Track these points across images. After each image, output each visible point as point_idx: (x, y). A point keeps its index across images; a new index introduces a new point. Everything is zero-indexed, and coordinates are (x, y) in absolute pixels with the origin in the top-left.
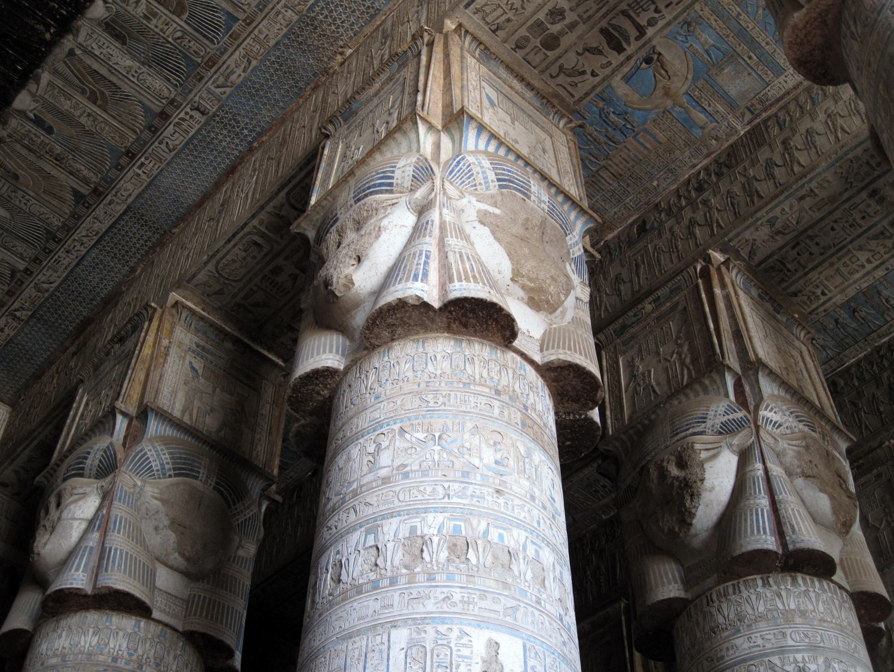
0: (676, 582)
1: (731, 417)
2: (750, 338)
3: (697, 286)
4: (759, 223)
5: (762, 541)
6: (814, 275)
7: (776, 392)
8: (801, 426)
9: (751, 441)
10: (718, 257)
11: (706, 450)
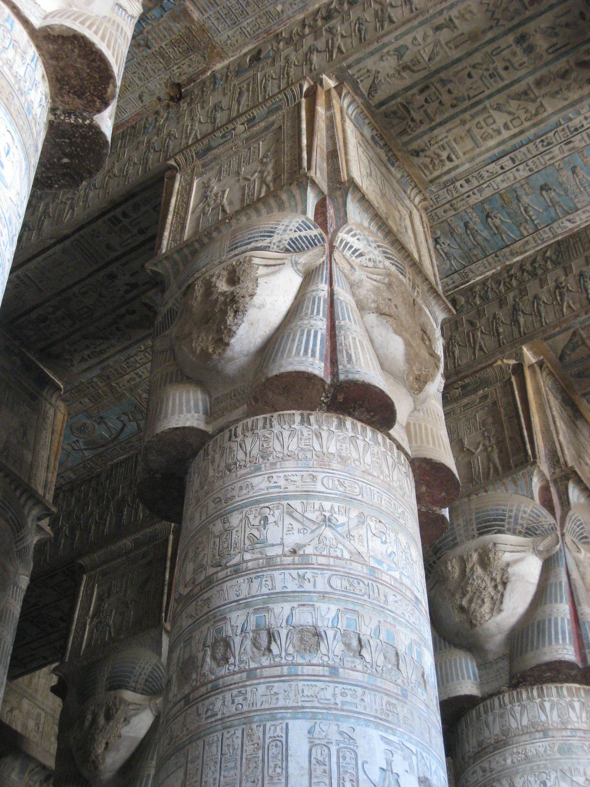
0: (197, 412)
1: (303, 234)
2: (347, 162)
3: (299, 105)
4: (385, 50)
5: (307, 364)
6: (440, 132)
7: (366, 224)
8: (387, 263)
9: (321, 260)
10: (331, 83)
11: (266, 265)
